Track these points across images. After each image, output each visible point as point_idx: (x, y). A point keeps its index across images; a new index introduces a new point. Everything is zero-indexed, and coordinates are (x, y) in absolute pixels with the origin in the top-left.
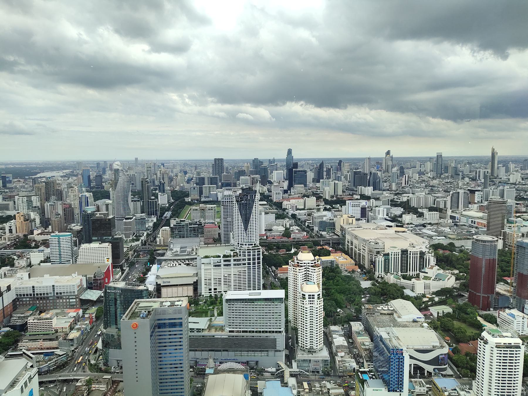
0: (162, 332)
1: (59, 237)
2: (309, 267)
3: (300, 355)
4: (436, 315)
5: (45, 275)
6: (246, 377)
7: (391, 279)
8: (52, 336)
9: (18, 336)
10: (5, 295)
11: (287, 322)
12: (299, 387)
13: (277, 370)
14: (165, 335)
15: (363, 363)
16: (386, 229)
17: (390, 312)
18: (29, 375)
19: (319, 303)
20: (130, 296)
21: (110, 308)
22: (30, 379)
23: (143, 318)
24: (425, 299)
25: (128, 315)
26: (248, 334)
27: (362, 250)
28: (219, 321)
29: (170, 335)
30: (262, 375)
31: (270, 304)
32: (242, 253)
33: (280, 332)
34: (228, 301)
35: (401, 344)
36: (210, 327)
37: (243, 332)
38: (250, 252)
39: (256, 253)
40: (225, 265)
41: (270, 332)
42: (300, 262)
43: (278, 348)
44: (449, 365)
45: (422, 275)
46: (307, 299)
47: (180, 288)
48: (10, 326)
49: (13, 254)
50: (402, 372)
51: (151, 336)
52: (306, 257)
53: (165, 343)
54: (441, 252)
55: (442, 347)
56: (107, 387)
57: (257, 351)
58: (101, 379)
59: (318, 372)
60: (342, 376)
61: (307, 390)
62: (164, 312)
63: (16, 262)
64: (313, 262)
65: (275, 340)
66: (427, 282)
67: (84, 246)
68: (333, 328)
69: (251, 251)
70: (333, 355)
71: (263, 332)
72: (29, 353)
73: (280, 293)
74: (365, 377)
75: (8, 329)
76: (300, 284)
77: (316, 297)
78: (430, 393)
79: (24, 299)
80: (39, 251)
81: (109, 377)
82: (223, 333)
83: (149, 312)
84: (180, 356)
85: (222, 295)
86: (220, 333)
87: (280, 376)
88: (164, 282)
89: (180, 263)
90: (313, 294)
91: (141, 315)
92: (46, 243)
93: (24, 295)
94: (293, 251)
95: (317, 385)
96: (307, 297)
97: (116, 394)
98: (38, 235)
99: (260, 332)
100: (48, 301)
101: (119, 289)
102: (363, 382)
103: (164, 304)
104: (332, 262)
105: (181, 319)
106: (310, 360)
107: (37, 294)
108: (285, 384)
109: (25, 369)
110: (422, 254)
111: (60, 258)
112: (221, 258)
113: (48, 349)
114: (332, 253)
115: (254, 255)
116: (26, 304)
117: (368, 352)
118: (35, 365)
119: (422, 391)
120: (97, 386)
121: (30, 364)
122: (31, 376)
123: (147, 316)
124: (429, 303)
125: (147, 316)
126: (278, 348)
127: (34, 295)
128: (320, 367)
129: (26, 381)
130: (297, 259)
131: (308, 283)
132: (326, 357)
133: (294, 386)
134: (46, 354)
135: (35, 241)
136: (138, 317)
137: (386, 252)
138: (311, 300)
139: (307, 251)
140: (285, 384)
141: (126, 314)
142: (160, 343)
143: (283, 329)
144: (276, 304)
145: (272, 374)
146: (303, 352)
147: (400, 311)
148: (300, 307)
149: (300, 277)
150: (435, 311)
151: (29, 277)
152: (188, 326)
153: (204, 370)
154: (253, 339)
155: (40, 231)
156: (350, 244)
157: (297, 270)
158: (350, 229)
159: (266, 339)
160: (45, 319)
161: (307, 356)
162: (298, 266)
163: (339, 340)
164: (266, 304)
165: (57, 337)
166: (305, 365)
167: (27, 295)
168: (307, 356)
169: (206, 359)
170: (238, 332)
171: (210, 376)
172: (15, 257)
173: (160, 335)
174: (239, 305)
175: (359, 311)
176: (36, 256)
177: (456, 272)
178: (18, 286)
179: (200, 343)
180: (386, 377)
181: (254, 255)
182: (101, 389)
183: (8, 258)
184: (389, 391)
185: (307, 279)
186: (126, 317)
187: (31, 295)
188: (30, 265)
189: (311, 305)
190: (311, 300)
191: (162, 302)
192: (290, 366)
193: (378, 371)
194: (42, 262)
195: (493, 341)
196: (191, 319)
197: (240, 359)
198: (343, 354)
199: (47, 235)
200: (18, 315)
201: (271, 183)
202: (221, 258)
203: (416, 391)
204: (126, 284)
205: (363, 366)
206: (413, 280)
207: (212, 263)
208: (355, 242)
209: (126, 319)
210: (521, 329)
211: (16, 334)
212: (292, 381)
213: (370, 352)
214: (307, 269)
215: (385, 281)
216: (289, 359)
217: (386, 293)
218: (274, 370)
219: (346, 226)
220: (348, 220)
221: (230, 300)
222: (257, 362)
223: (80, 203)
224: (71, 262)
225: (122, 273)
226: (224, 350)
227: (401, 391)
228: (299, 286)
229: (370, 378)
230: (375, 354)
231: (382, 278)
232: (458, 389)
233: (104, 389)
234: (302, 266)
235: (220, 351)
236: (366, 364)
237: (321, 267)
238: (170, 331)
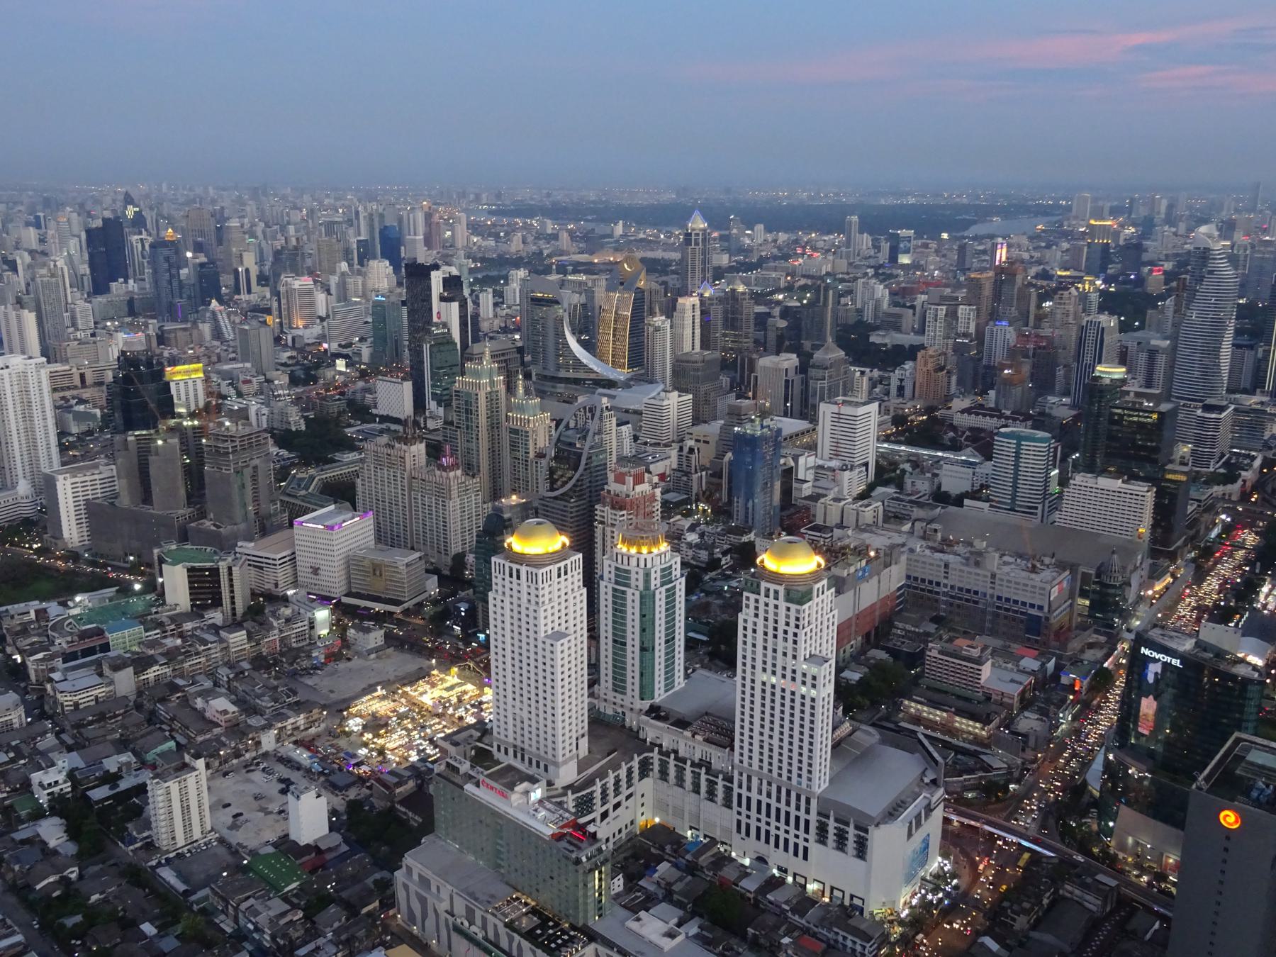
1: (1019, 438)
8: (978, 706)
18: (926, 802)
22: (929, 810)
48: (888, 650)
58: (1089, 880)
63: (908, 481)
67: (1079, 479)
75: (882, 655)
81: (1113, 883)
98: (963, 412)
120: (1077, 892)
122: (929, 804)
129: (920, 814)
135: (953, 428)
136: (1248, 795)
155: (966, 403)
165: (988, 715)
172: (907, 466)
182: (1087, 904)
186: (1207, 779)
199: (985, 415)
223: (1081, 341)
224: (1039, 511)
233: (1094, 908)
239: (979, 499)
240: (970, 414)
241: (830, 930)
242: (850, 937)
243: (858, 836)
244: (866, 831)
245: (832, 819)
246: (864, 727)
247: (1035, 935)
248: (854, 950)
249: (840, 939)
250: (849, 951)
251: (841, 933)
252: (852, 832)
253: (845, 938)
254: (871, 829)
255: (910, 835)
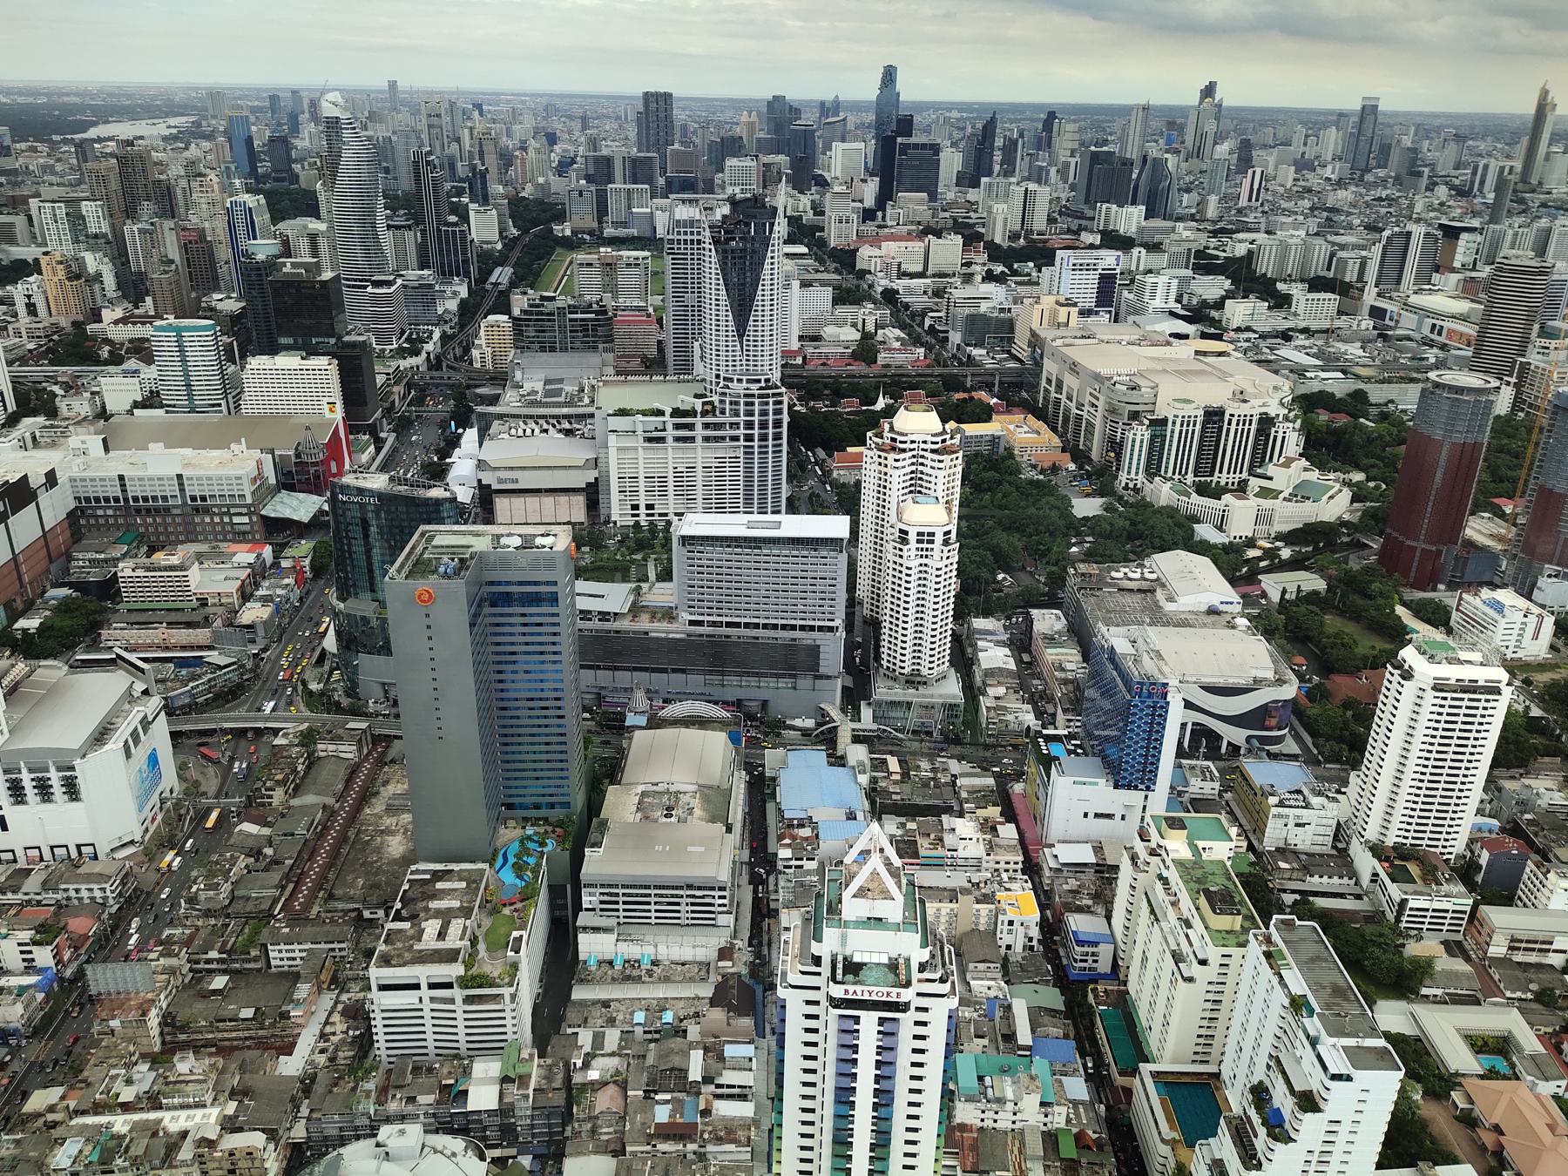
0: (502, 615)
2: (926, 454)
3: (883, 691)
4: (1275, 597)
5: (151, 445)
6: (735, 739)
7: (1163, 493)
8: (196, 614)
9: (96, 612)
10: (44, 498)
11: (852, 602)
12: (874, 768)
13: (819, 725)
14: (510, 625)
15: (1054, 715)
16: (1168, 344)
17: (1145, 585)
19: (946, 554)
20: (406, 515)
21: (350, 545)
22: (146, 723)
23: (446, 576)
24: (1252, 553)
25: (402, 565)
26: (742, 631)
27: (1087, 408)
28: (661, 594)
29: (525, 625)
30: (778, 735)
31: (805, 553)
32: (727, 406)
33: (831, 629)
34: (686, 540)
35: (1166, 669)
36: (636, 610)
37: (729, 625)
38: (753, 404)
39: (771, 407)
40: (677, 439)
41: (802, 628)
42: (900, 438)
43: (822, 670)
44: (1292, 729)
45: (1255, 483)
46: (913, 544)
47: (548, 501)
48: (70, 585)
49: (49, 379)
50: (1160, 740)
51: (472, 625)
52: (918, 422)
53: (513, 644)
54: (1323, 417)
55: (1280, 682)
56: (360, 750)
57: (765, 675)
58: (340, 731)
59: (929, 734)
60: (994, 746)
61: (898, 777)
62: (505, 562)
63: (62, 405)
64: (939, 439)
65: (814, 651)
66: (1267, 503)
67: (256, 362)
68: (979, 623)
69: (757, 401)
70: (972, 692)
71: (784, 627)
72: (132, 657)
73: (836, 526)
74: (1057, 749)
75: (65, 591)
76: (894, 501)
77: (939, 538)
78: (1228, 796)
79: (100, 512)
80: (124, 372)
81: (364, 725)
82: (673, 627)
83: (461, 560)
84: (556, 681)
85: (669, 523)
86: (664, 625)
87: (826, 738)
88: (500, 481)
89: (545, 426)
90: (931, 530)
91: (442, 569)
92: (142, 350)
93: (97, 500)
94: (881, 404)
95: (924, 764)
96: (912, 537)
97: (386, 769)
98: (116, 322)
99: (775, 627)
100: (169, 520)
101: (371, 493)
102: (1047, 762)
103: (503, 541)
104: (994, 440)
105: (555, 583)
106: (909, 704)
107: (136, 499)
108: (838, 760)
109: (129, 697)
110: (1266, 422)
111: (190, 395)
112: (667, 418)
113: (184, 648)
114: (998, 413)
115: (764, 413)
116: (108, 526)
117: (1070, 687)
118: (154, 688)
119: (1207, 791)
121: (140, 687)
122: (145, 717)
123: (457, 572)
124: (1263, 564)
125: (457, 572)
126: (822, 670)
127: (126, 500)
128: (937, 722)
129: (136, 729)
130: (892, 430)
131: (920, 498)
132: (954, 697)
133: (861, 764)
134: (182, 663)
135: (107, 341)
136: (435, 572)
137: (1159, 414)
138: (925, 546)
139: (923, 406)
140: (838, 760)
141: (397, 564)
142: (498, 644)
143: (838, 622)
144: (825, 553)
145: (806, 733)
146: (891, 683)
147: (1175, 584)
148: (891, 565)
149: (895, 480)
150: (1274, 586)
151: (107, 450)
152: (574, 605)
153: (623, 717)
154: (755, 644)
155: (119, 313)
156: (1052, 389)
157: (890, 462)
158: (1059, 342)
159: (792, 647)
160: (166, 568)
161: (899, 693)
162: (894, 449)
163: (994, 656)
164: (795, 553)
165: (206, 618)
166: (894, 714)
167: (107, 500)
168: (899, 693)
169: (626, 690)
170: (714, 624)
171: (637, 733)
172: (56, 389)
173: (498, 625)
174: (718, 553)
175: (1058, 580)
176: (118, 389)
177: (1358, 477)
178: (75, 472)
179: (607, 648)
180: (1112, 752)
181: (764, 413)
183: (37, 391)
184: (1116, 787)
185: (917, 487)
186: (399, 571)
187: (117, 500)
188: (103, 414)
189: (924, 561)
190: (925, 546)
191: (498, 537)
192: (857, 717)
193: (1090, 736)
194: (136, 405)
195: (1425, 671)
196: (582, 586)
197: (718, 693)
198: (1001, 691)
199: (143, 323)
200: (89, 556)
201: (823, 183)
202: (667, 418)
203: (1191, 789)
204: (392, 479)
205: (1053, 724)
206: (1227, 498)
207: (639, 432)
208: (1070, 381)
209: (400, 578)
210: (1512, 644)
211: (91, 606)
212: (858, 754)
213: (1078, 688)
214: (918, 460)
215: (1143, 498)
216: (853, 698)
217: (1146, 531)
218: (810, 723)
219: (1046, 333)
220: (1054, 314)
221: (693, 537)
222: (765, 704)
223: (231, 227)
224: (224, 408)
225: (378, 450)
226: (674, 671)
227: (1148, 788)
228: (893, 507)
229: (1069, 752)
230: (1090, 693)
231: (1136, 490)
232: (1306, 792)
234: (904, 450)
235: (664, 671)
236: (1061, 717)
237: (960, 454)
238: (524, 615)
239: (151, 407)
240: (125, 324)
241: (56, 890)
242: (83, 887)
243: (65, 778)
244: (72, 768)
245: (24, 771)
246: (43, 663)
247: (295, 802)
248: (93, 899)
249: (72, 894)
250: (87, 901)
251: (71, 887)
252: (55, 778)
253: (77, 891)
254: (77, 762)
255: (128, 754)
